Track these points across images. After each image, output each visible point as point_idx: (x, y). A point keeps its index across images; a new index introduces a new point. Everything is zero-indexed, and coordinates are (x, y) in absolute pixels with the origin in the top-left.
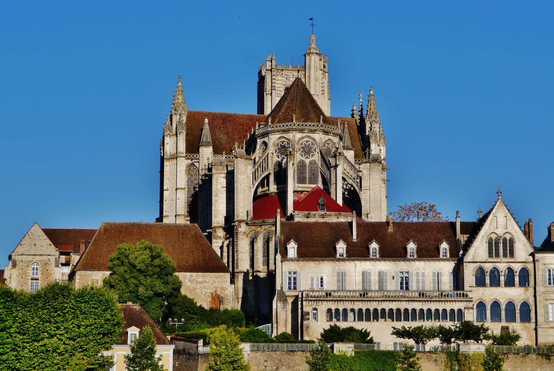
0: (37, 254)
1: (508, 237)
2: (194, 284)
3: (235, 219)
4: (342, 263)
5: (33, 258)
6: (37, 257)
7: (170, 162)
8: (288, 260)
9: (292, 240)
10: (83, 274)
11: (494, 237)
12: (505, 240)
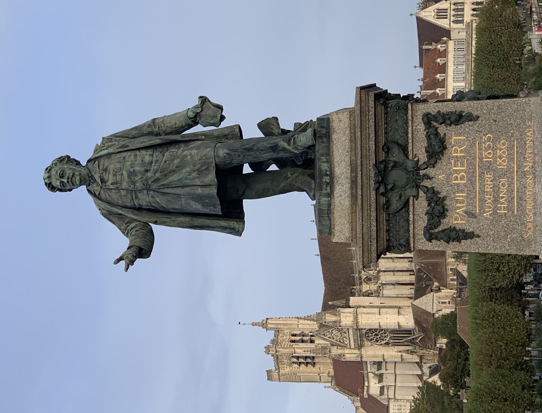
0: (432, 302)
1: (436, 11)
4: (448, 90)
5: (435, 304)
6: (434, 302)
10: (448, 257)
11: (436, 16)
12: (437, 12)
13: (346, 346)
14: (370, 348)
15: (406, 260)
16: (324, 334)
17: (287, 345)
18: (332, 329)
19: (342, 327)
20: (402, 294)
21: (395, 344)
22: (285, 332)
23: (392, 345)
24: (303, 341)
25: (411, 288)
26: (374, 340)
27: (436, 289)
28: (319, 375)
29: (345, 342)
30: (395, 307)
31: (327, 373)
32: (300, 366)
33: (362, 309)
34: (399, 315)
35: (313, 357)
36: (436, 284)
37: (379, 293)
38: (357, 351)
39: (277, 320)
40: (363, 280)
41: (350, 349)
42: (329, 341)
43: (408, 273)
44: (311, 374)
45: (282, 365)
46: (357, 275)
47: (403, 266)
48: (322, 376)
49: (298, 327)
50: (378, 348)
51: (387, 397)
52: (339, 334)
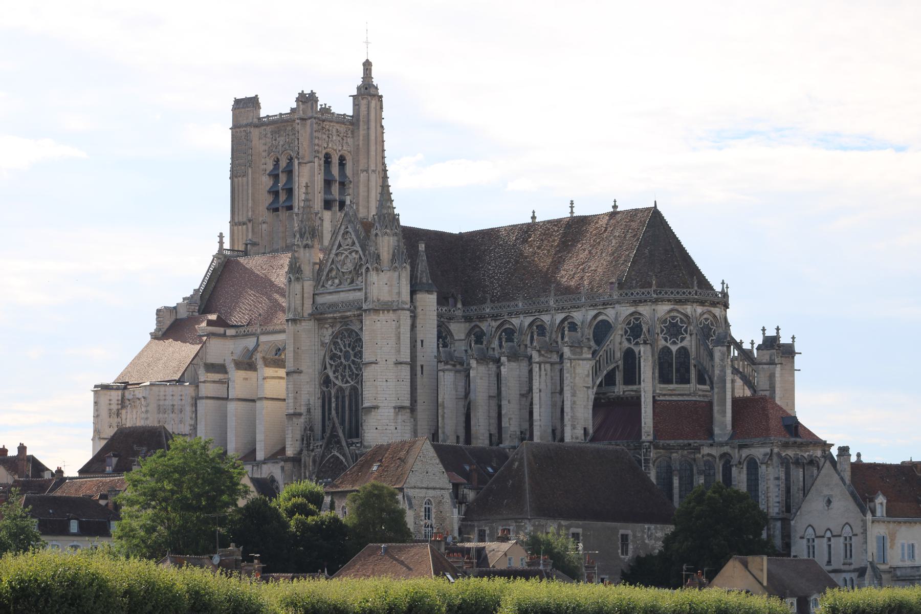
0: (430, 486)
2: (653, 542)
3: (644, 438)
6: (430, 491)
7: (381, 315)
8: (878, 522)
9: (879, 492)
10: (537, 523)
13: (321, 284)
14: (317, 340)
15: (526, 426)
16: (347, 232)
17: (318, 145)
18: (361, 252)
19: (366, 276)
20: (446, 416)
21: (325, 400)
22: (350, 141)
23: (323, 393)
24: (328, 183)
25: (458, 437)
26: (334, 351)
27: (460, 496)
28: (250, 221)
29: (330, 282)
30: (414, 400)
31: (254, 240)
32: (269, 175)
33: (409, 322)
34: (395, 408)
35: (290, 208)
36: (471, 495)
37: (446, 363)
38: (308, 309)
39: (378, 121)
40: (478, 323)
41: (313, 294)
42: (333, 245)
43: (494, 431)
44: (250, 201)
45: (272, 132)
46: (488, 310)
47: (510, 419)
48: (247, 228)
49: (363, 171)
50: (317, 359)
51: (202, 380)
52: (349, 266)
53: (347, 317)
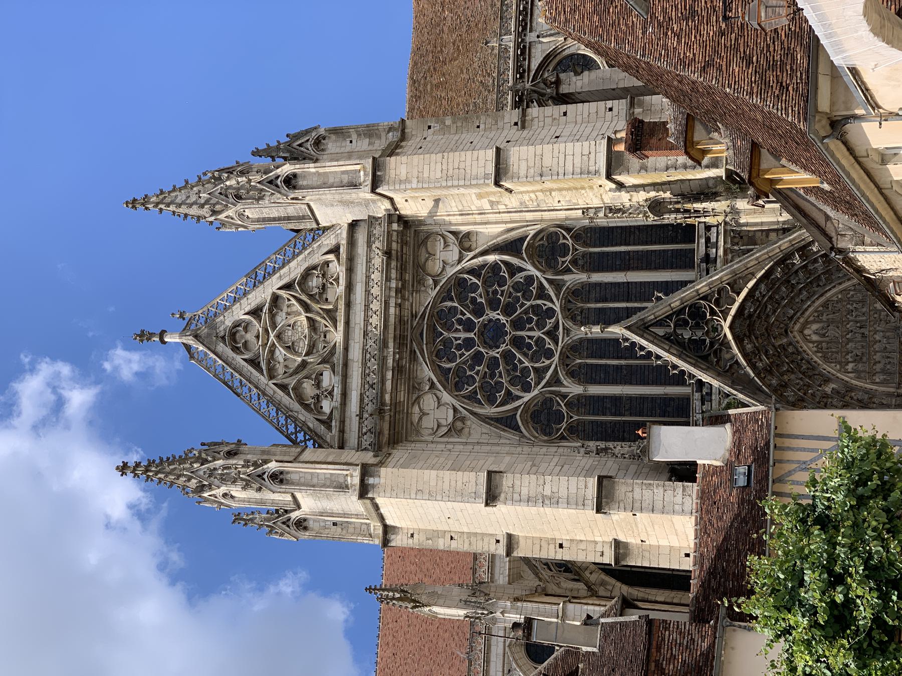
14: (441, 447)
53: (400, 320)
